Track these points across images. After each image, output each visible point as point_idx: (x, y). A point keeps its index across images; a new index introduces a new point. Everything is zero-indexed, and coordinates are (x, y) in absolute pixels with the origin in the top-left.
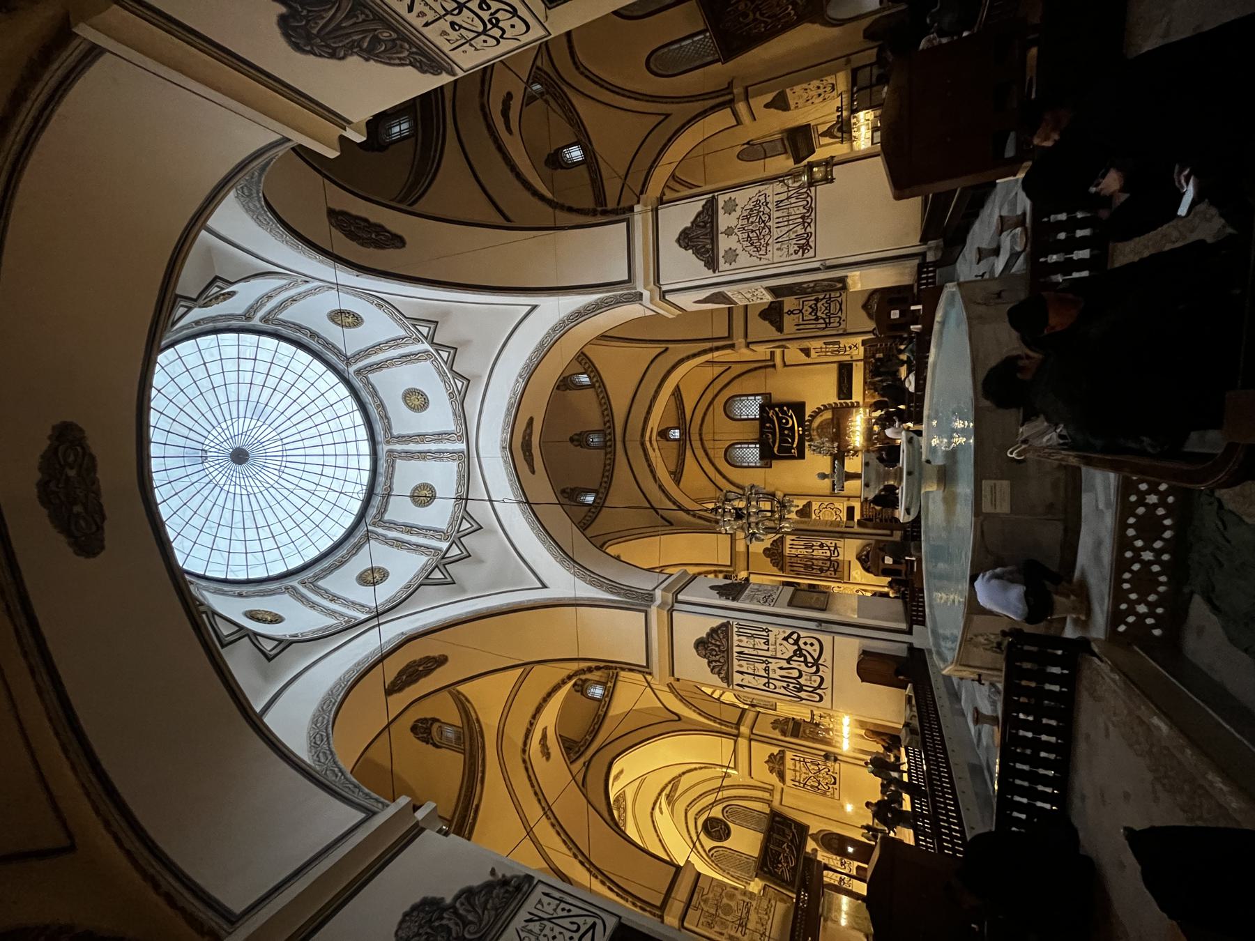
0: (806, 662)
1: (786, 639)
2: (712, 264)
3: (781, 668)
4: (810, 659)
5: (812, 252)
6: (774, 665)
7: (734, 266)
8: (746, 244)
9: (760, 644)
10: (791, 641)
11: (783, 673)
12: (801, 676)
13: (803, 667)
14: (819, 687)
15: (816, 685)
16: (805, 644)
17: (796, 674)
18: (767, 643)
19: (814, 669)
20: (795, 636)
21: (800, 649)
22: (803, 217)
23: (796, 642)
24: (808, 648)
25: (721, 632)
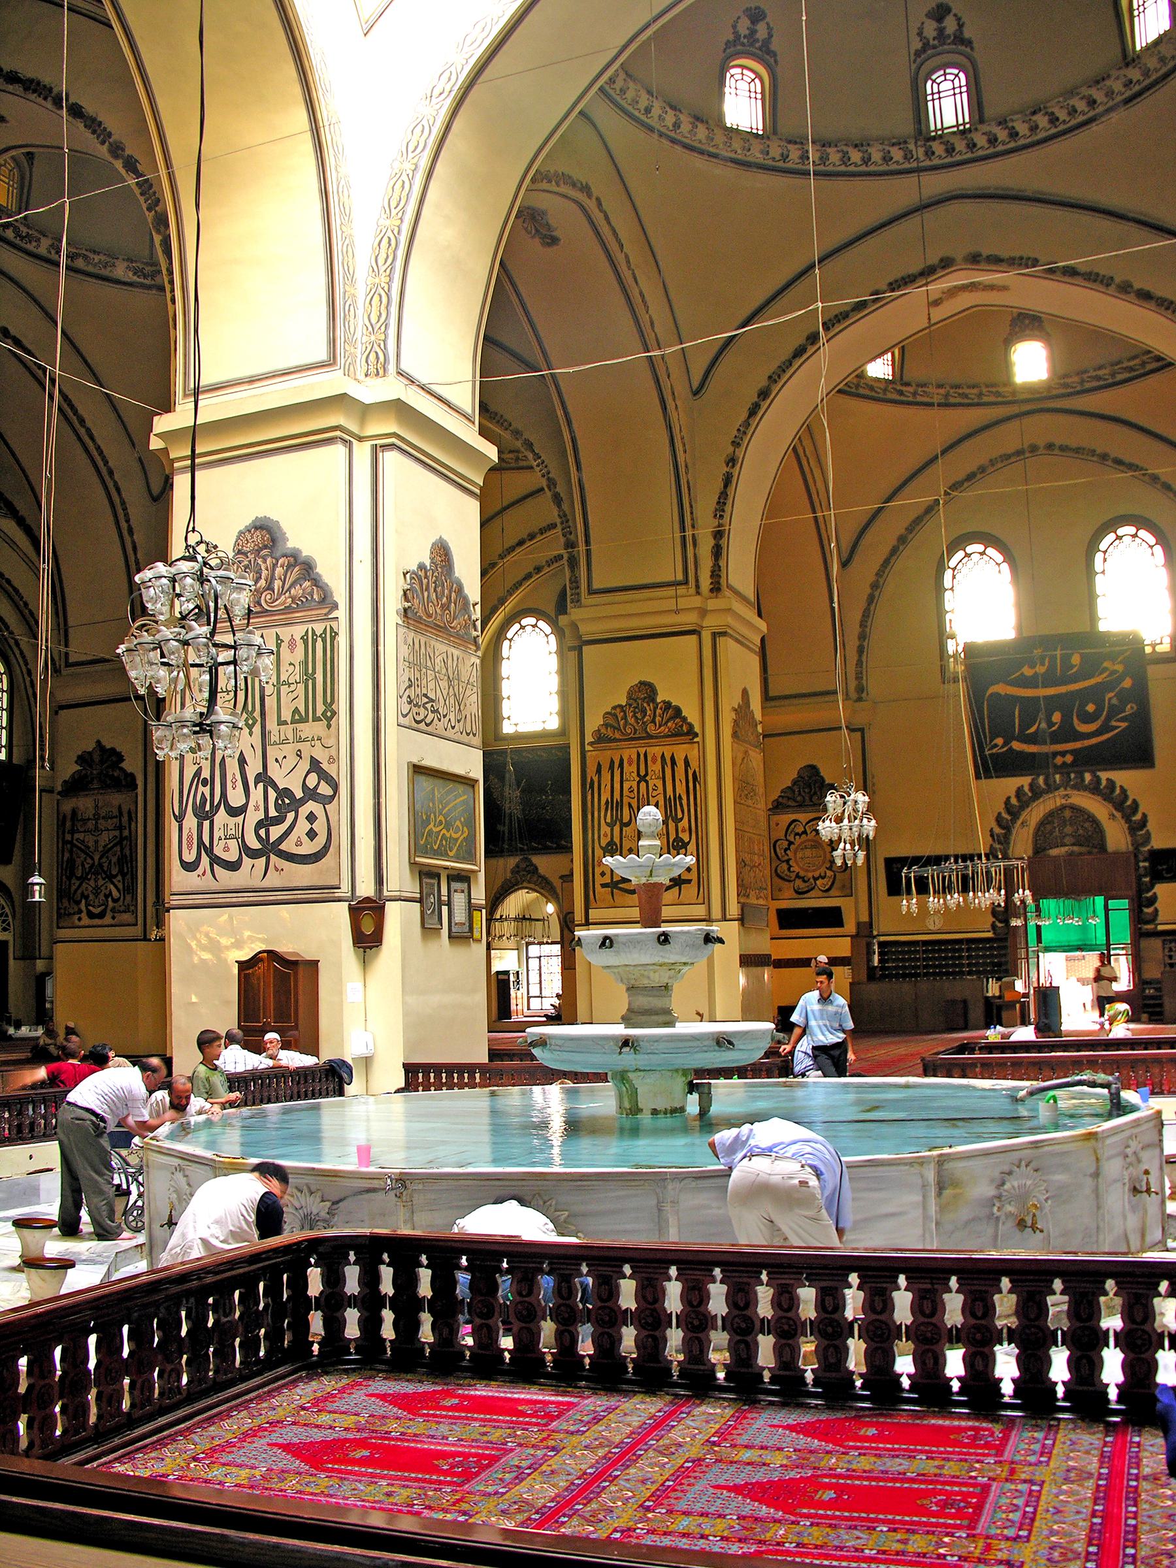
0: (265, 823)
1: (315, 766)
3: (242, 761)
4: (276, 832)
9: (292, 700)
11: (233, 768)
12: (234, 812)
13: (254, 816)
14: (215, 860)
15: (218, 851)
16: (311, 818)
17: (236, 798)
18: (299, 718)
19: (254, 844)
20: (325, 789)
21: (297, 804)
23: (311, 794)
24: (303, 826)
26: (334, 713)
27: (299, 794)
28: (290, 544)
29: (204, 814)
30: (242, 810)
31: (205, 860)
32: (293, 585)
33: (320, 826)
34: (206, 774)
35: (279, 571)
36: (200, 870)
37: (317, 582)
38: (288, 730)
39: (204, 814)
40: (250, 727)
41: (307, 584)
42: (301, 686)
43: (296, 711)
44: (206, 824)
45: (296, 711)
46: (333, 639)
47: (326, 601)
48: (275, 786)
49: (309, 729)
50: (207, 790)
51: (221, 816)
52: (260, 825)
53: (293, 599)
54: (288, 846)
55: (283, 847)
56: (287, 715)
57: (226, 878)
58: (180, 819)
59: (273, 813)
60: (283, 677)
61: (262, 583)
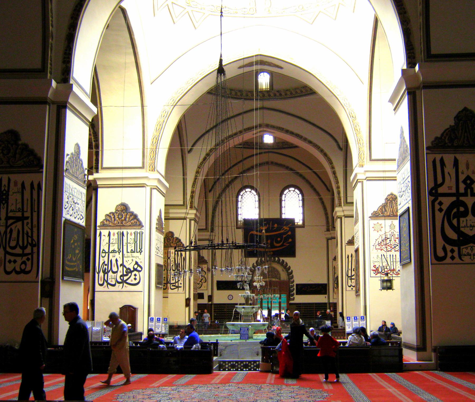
0: (123, 276)
1: (137, 263)
2: (375, 216)
3: (117, 260)
4: (125, 278)
5: (374, 275)
6: (118, 256)
7: (372, 229)
8: (384, 237)
10: (136, 266)
11: (114, 262)
12: (114, 272)
13: (119, 274)
14: (108, 284)
15: (109, 281)
16: (135, 275)
17: (115, 269)
18: (132, 252)
19: (120, 280)
20: (139, 269)
21: (131, 272)
22: (394, 270)
23: (135, 270)
24: (133, 277)
25: (135, 221)
26: (142, 251)
27: (132, 269)
28: (131, 210)
29: (105, 272)
30: (116, 272)
31: (105, 284)
32: (132, 220)
33: (137, 277)
34: (106, 263)
35: (128, 216)
36: (104, 286)
37: (138, 220)
38: (130, 254)
39: (105, 272)
40: (119, 253)
41: (135, 220)
42: (133, 245)
43: (132, 250)
44: (106, 275)
45: (132, 250)
46: (142, 234)
47: (140, 225)
48: (126, 267)
49: (135, 254)
50: (106, 267)
51: (110, 273)
52: (121, 276)
53: (132, 223)
54: (129, 281)
55: (128, 281)
56: (129, 251)
57: (111, 288)
58: (99, 273)
59: (125, 273)
60: (128, 242)
61: (123, 219)
